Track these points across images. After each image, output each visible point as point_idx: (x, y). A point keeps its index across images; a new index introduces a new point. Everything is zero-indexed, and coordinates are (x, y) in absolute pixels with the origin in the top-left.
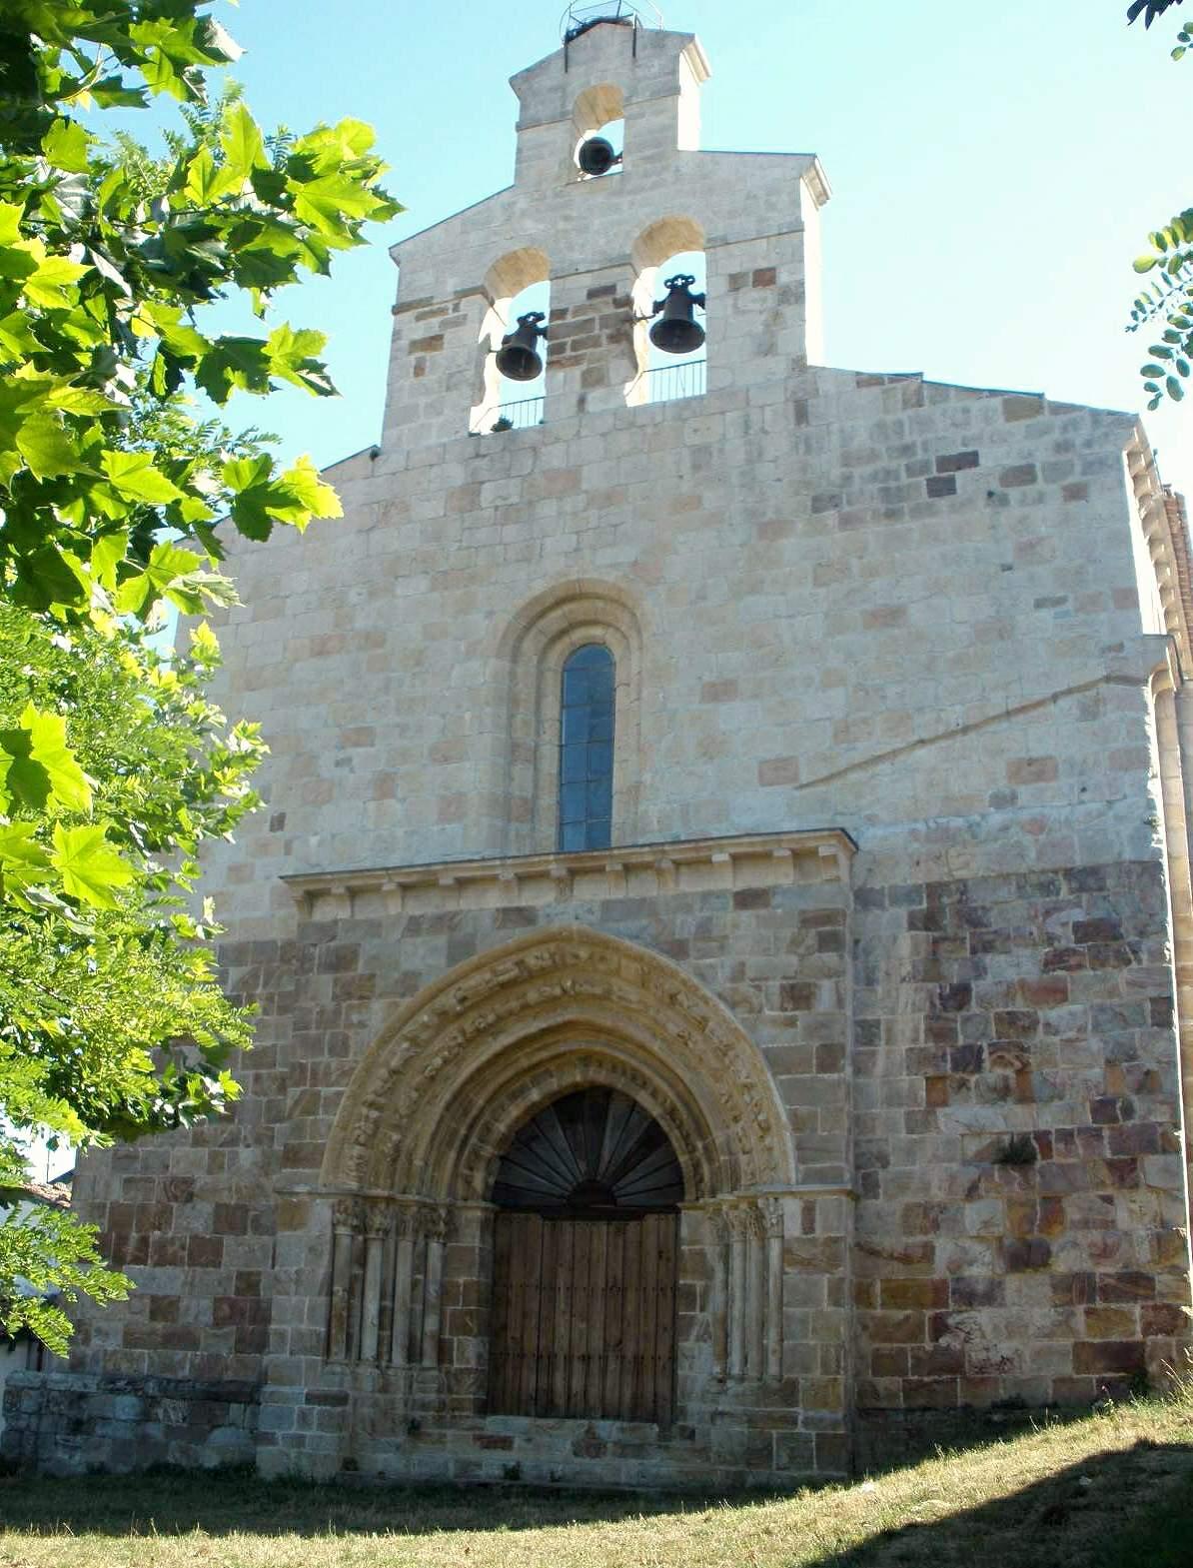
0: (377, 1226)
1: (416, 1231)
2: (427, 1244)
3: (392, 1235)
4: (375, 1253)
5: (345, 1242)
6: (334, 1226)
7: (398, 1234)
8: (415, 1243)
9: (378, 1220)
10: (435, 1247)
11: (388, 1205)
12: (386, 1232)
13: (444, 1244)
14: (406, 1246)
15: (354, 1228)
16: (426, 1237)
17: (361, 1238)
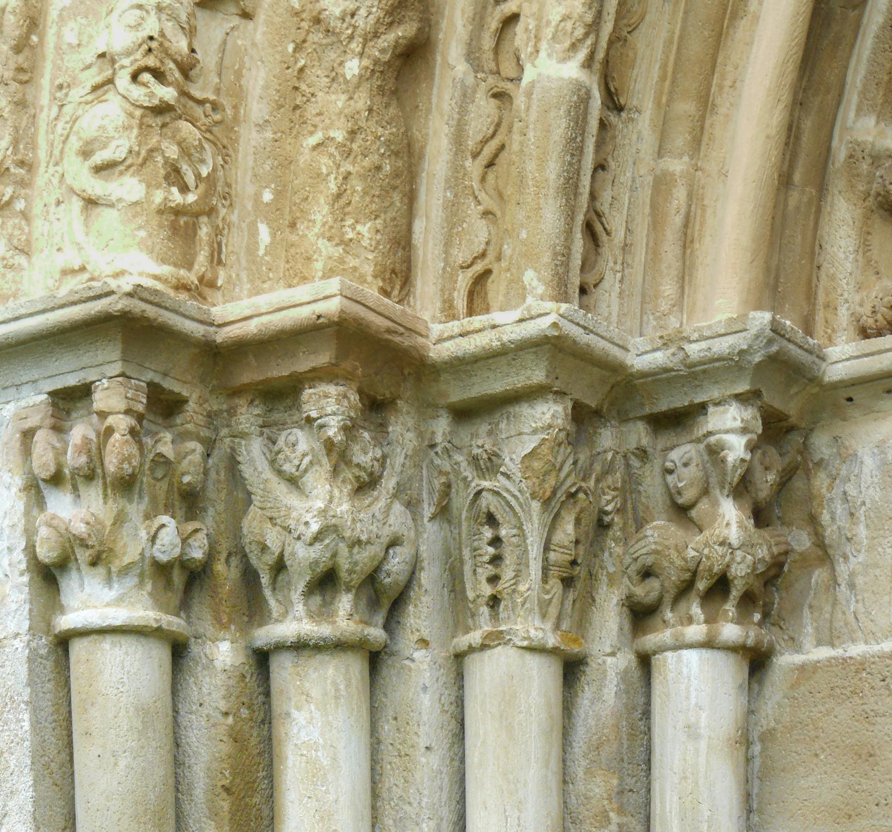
0: (304, 556)
1: (573, 579)
2: (645, 661)
3: (422, 616)
4: (317, 719)
5: (119, 680)
6: (48, 576)
7: (458, 608)
8: (572, 669)
9: (304, 503)
10: (696, 683)
11: (375, 408)
12: (387, 600)
13: (757, 661)
14: (511, 686)
15: (184, 581)
16: (641, 615)
17: (223, 653)
